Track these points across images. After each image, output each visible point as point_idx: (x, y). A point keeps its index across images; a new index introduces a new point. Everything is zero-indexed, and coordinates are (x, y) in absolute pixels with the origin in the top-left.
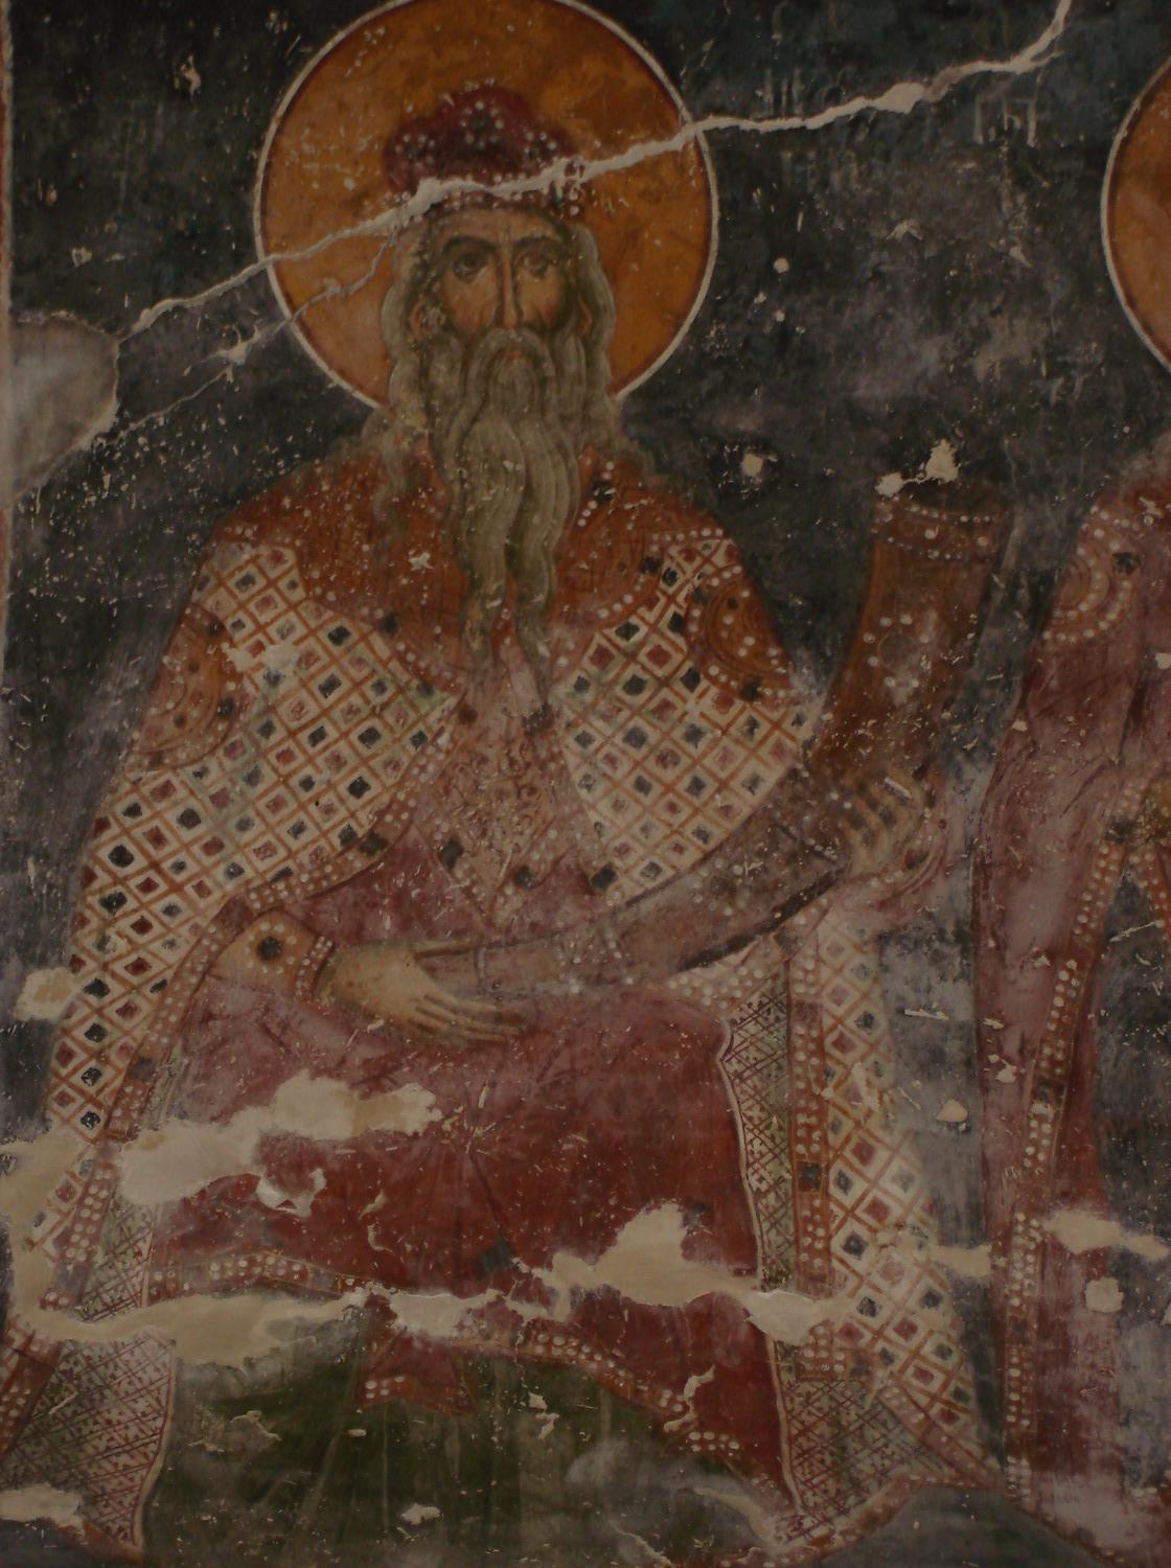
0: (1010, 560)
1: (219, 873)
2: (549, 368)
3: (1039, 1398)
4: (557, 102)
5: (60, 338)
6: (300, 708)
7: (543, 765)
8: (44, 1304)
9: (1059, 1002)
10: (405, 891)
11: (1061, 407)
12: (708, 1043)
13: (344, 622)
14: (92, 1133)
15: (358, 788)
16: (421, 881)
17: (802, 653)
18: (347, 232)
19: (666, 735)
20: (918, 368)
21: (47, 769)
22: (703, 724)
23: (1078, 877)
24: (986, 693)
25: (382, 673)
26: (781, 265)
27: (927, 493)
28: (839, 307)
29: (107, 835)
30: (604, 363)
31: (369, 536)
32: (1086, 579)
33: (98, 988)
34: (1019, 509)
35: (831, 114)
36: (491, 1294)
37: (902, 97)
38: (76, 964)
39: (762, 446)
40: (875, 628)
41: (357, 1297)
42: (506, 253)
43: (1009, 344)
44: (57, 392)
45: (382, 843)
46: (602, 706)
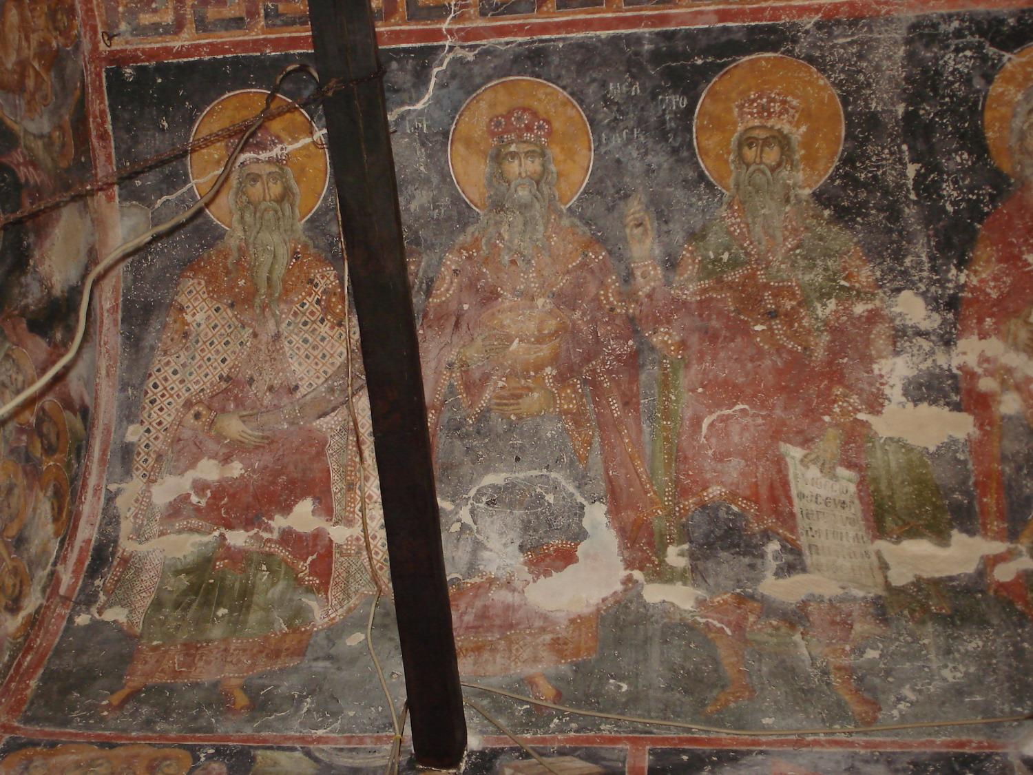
0: (421, 274)
1: (184, 390)
2: (280, 213)
5: (135, 210)
6: (206, 334)
7: (278, 351)
11: (437, 220)
12: (323, 443)
13: (219, 305)
15: (224, 361)
16: (242, 391)
21: (134, 357)
22: (325, 335)
23: (437, 382)
25: (230, 322)
30: (297, 211)
32: (444, 279)
33: (148, 431)
34: (424, 255)
36: (256, 530)
38: (142, 422)
41: (216, 533)
42: (265, 177)
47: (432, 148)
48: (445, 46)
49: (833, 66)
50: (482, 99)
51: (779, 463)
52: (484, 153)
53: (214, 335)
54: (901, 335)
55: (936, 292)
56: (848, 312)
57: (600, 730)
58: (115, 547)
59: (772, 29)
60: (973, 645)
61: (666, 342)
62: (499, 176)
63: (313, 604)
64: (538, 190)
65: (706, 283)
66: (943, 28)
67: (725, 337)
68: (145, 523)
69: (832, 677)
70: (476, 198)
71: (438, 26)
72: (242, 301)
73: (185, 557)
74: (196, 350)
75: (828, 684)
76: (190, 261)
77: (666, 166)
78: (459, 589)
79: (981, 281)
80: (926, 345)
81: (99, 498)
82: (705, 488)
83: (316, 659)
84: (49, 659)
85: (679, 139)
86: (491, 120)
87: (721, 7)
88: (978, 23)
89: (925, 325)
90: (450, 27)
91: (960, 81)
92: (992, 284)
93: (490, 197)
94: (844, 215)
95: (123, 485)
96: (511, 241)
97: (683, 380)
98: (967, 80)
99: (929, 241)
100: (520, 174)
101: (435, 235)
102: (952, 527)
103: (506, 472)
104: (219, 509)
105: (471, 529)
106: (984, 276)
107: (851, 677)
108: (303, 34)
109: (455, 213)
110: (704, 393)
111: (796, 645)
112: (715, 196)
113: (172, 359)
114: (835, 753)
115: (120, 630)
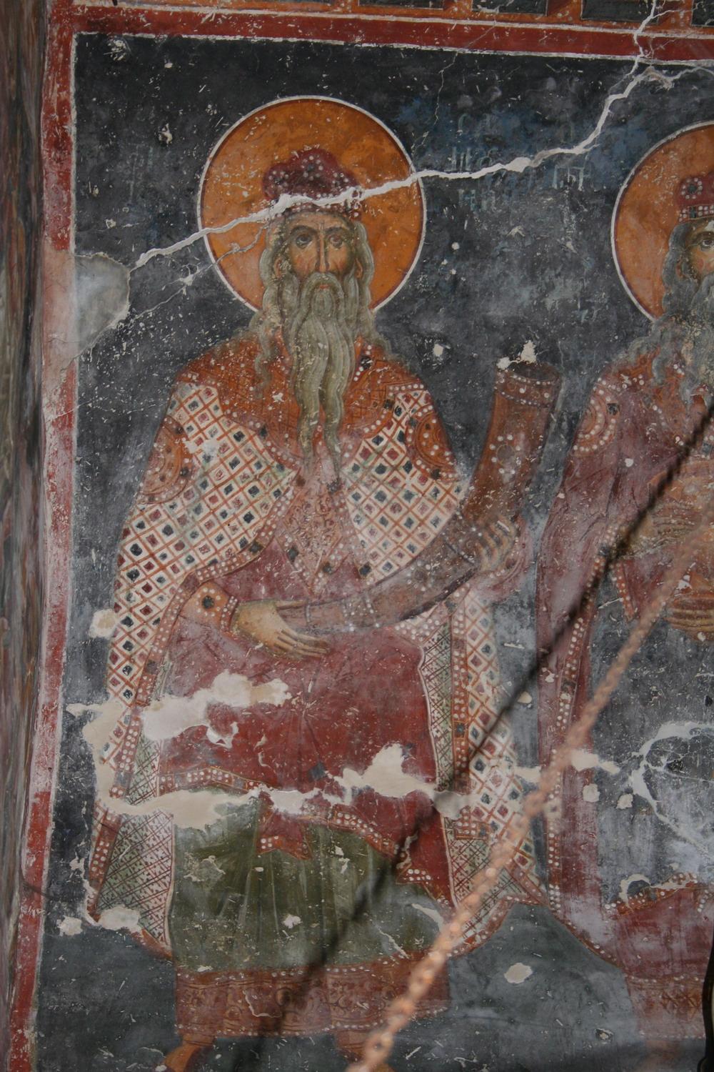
0: (559, 406)
1: (183, 560)
2: (341, 293)
3: (562, 850)
4: (350, 159)
5: (100, 266)
7: (337, 509)
8: (112, 794)
9: (574, 640)
10: (271, 573)
11: (586, 324)
12: (414, 659)
13: (241, 429)
14: (129, 701)
15: (248, 518)
16: (279, 568)
17: (461, 455)
18: (243, 220)
19: (395, 496)
20: (519, 301)
21: (99, 501)
22: (413, 490)
24: (546, 478)
25: (260, 458)
26: (456, 246)
27: (521, 368)
28: (482, 269)
29: (128, 538)
30: (368, 293)
31: (253, 382)
32: (594, 417)
34: (564, 378)
35: (484, 171)
36: (316, 791)
37: (519, 164)
38: (117, 608)
39: (444, 340)
40: (496, 442)
41: (255, 792)
42: (322, 235)
43: (564, 290)
44: (99, 296)
45: (260, 547)
46: (366, 479)
48: (632, 63)
50: (674, 149)
52: (667, 231)
53: (232, 477)
58: (91, 806)
63: (433, 914)
68: (136, 769)
70: (648, 297)
71: (627, 31)
72: (279, 426)
73: (208, 828)
74: (202, 498)
76: (191, 355)
78: (649, 899)
81: (54, 726)
83: (470, 1004)
84: (39, 992)
86: (682, 182)
90: (645, 34)
93: (668, 298)
95: (93, 707)
96: (695, 368)
101: (581, 347)
103: (693, 719)
104: (253, 754)
105: (648, 805)
108: (418, 20)
109: (613, 318)
113: (163, 509)
115: (137, 946)
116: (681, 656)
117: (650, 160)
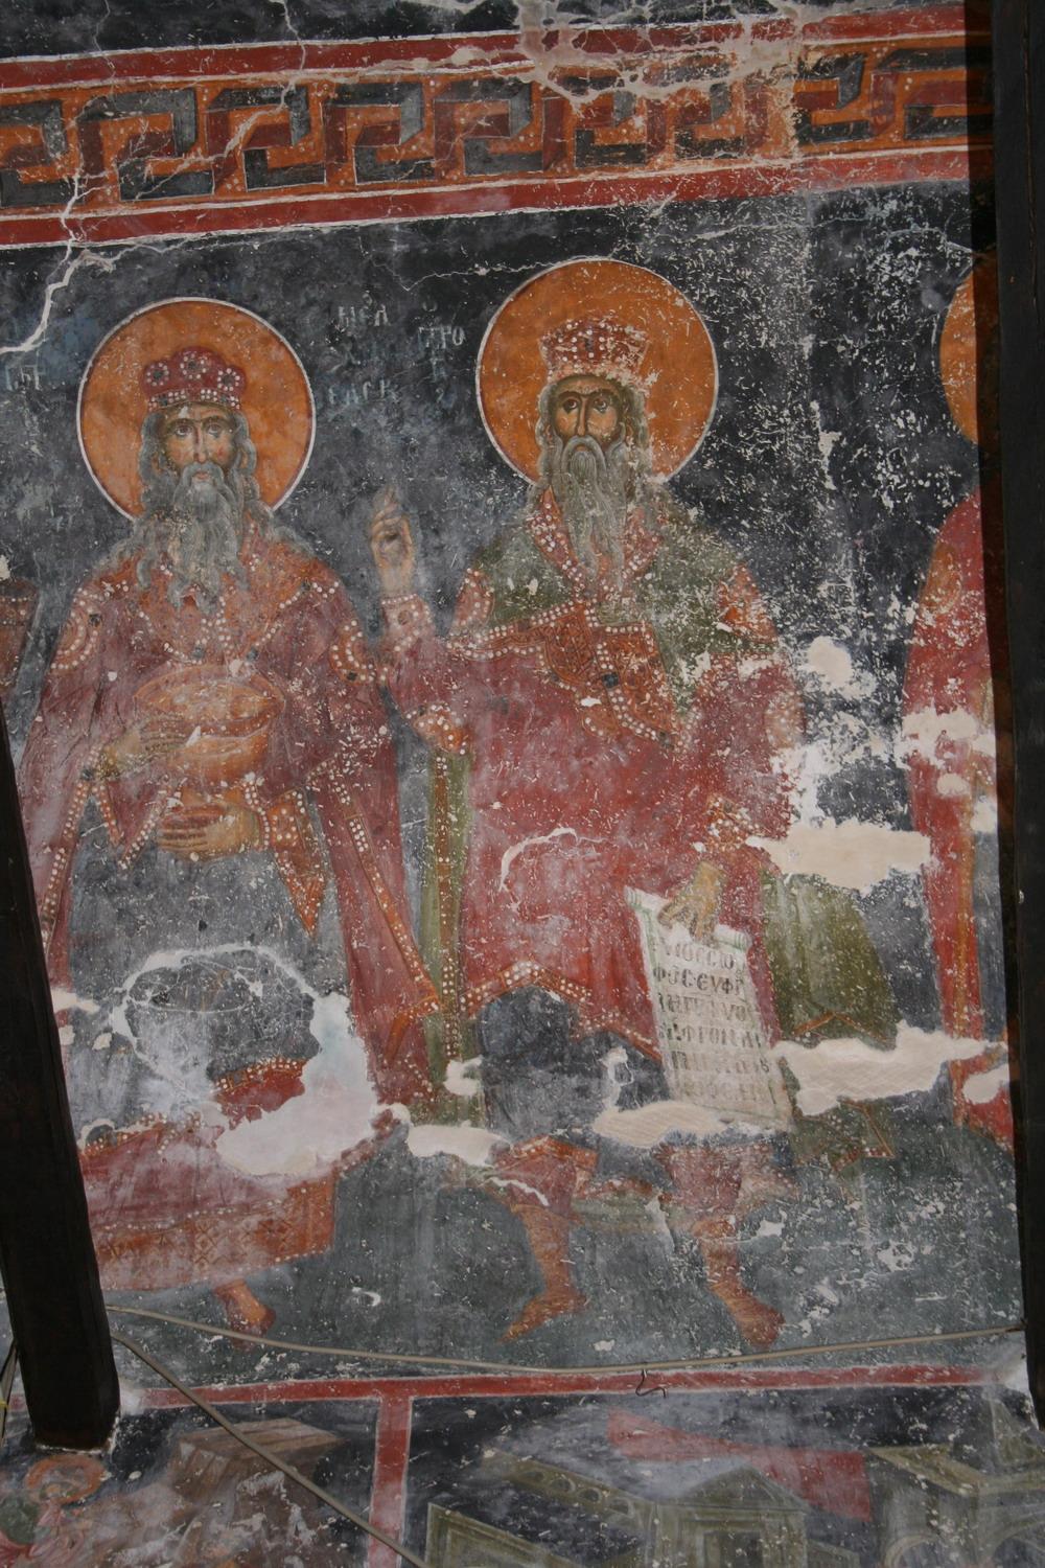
0: (36, 623)
9: (55, 872)
11: (62, 532)
23: (67, 802)
24: (22, 702)
32: (75, 631)
34: (41, 592)
47: (49, 416)
48: (65, 248)
49: (697, 276)
50: (131, 335)
51: (625, 921)
52: (138, 423)
54: (814, 709)
55: (869, 638)
56: (730, 673)
57: (335, 1372)
59: (597, 218)
60: (930, 1209)
61: (439, 728)
62: (161, 460)
64: (227, 482)
65: (503, 630)
66: (872, 211)
67: (535, 719)
69: (707, 1269)
70: (125, 496)
71: (53, 215)
75: (700, 1281)
77: (433, 439)
78: (108, 1145)
79: (938, 620)
80: (854, 724)
82: (507, 966)
85: (454, 397)
86: (146, 368)
87: (515, 182)
88: (928, 203)
89: (852, 693)
90: (73, 216)
91: (900, 297)
92: (957, 623)
93: (147, 495)
94: (721, 516)
96: (184, 566)
97: (469, 791)
98: (912, 295)
99: (856, 556)
100: (196, 455)
102: (899, 1018)
103: (185, 947)
105: (128, 1044)
106: (944, 610)
107: (736, 1268)
109: (90, 522)
110: (503, 810)
111: (650, 1219)
112: (514, 488)
114: (708, 1396)
116: (172, 879)
117: (107, 348)
